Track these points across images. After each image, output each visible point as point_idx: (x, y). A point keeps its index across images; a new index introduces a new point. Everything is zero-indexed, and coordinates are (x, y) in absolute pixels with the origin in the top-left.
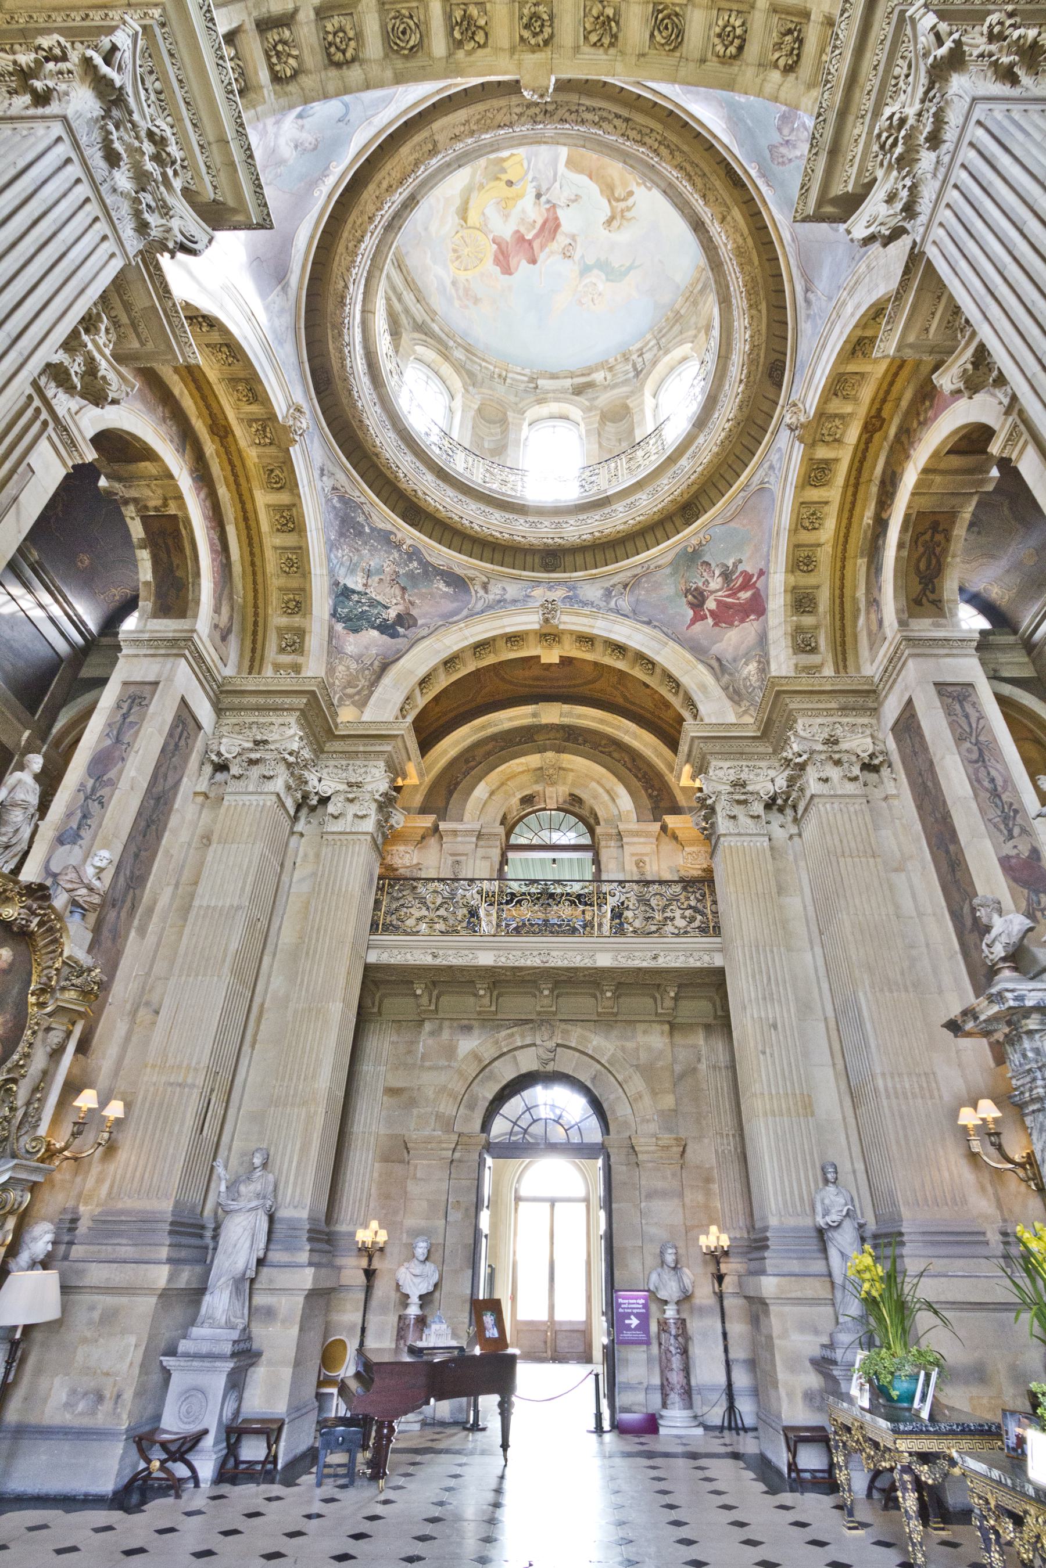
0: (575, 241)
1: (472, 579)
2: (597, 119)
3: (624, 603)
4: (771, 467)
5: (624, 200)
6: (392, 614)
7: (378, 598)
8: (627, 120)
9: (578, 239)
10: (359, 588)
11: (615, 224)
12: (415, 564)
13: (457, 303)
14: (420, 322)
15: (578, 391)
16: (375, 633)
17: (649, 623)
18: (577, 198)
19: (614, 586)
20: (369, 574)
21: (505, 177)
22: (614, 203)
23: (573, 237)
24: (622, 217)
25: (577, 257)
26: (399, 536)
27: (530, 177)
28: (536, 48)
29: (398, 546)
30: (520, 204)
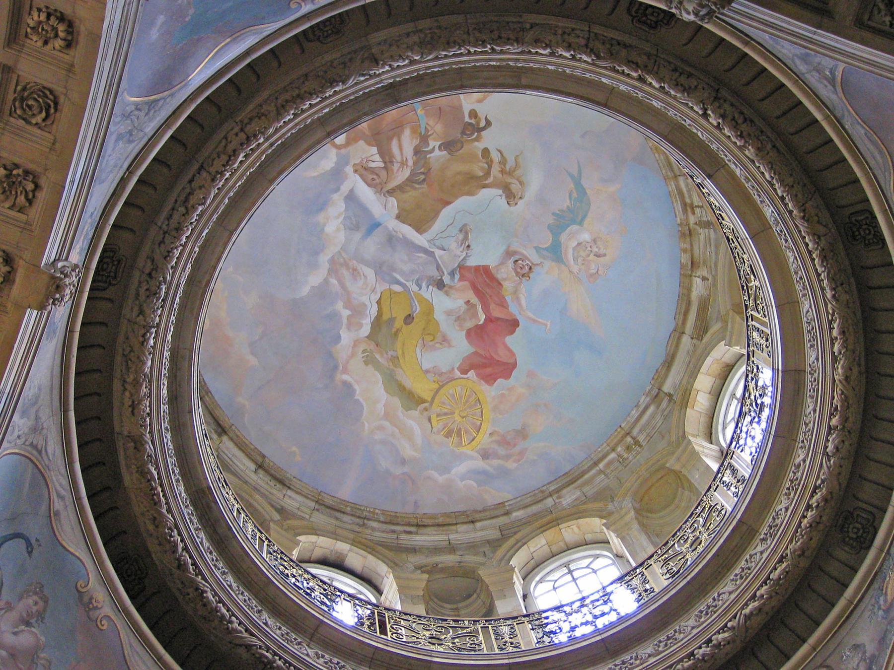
0: (515, 253)
2: (182, 210)
4: (805, 59)
5: (490, 164)
8: (202, 167)
9: (515, 247)
11: (515, 187)
13: (511, 465)
14: (496, 534)
15: (702, 329)
18: (464, 230)
21: (399, 323)
22: (490, 180)
23: (509, 254)
24: (510, 173)
25: (534, 257)
27: (415, 288)
30: (439, 315)
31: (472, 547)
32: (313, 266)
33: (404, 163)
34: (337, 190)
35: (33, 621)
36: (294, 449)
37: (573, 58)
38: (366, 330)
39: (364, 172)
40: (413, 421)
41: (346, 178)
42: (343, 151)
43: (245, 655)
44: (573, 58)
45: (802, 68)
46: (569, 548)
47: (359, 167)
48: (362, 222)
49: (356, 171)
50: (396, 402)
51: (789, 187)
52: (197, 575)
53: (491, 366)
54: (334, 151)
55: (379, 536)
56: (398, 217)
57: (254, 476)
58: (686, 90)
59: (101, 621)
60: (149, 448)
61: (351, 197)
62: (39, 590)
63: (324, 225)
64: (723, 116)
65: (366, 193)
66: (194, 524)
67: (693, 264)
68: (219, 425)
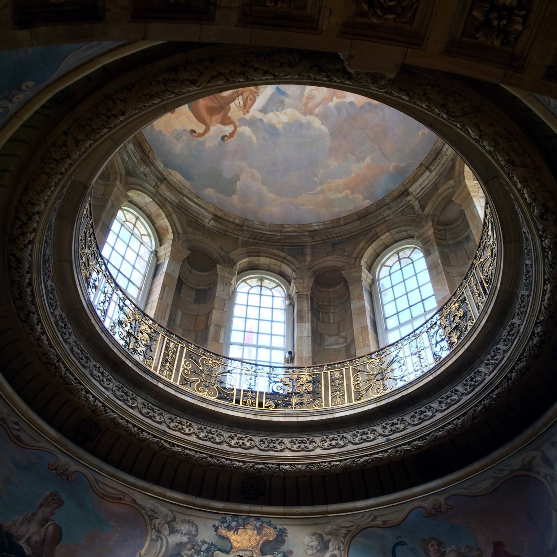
32: (309, 125)
34: (261, 120)
35: (443, 550)
36: (420, 133)
39: (247, 106)
41: (253, 116)
42: (237, 124)
47: (245, 111)
49: (248, 112)
52: (426, 439)
54: (239, 129)
57: (434, 173)
59: (448, 506)
61: (264, 110)
63: (283, 123)
68: (403, 193)
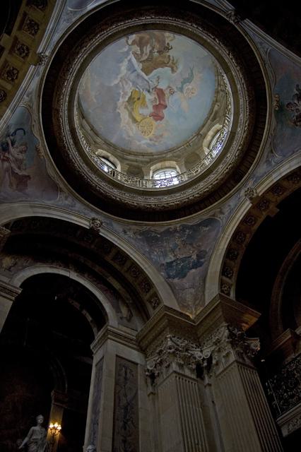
1: (214, 215)
3: (278, 157)
4: (261, 44)
5: (170, 59)
6: (194, 257)
7: (184, 256)
9: (171, 85)
10: (173, 259)
12: (188, 231)
13: (156, 144)
14: (149, 160)
15: (214, 119)
16: (194, 270)
17: (294, 152)
18: (158, 77)
19: (267, 157)
20: (173, 251)
21: (136, 100)
23: (169, 87)
25: (175, 90)
26: (172, 227)
28: (27, 55)
29: (175, 231)
30: (147, 100)
31: (142, 162)
33: (146, 54)
34: (126, 58)
37: (197, 28)
38: (127, 99)
40: (134, 127)
43: (77, 173)
44: (197, 28)
45: (259, 46)
46: (166, 168)
48: (131, 69)
50: (131, 120)
51: (246, 81)
53: (157, 116)
54: (127, 47)
55: (119, 154)
56: (142, 70)
58: (226, 45)
60: (61, 114)
61: (130, 61)
62: (26, 144)
64: (234, 56)
65: (134, 60)
66: (69, 137)
67: (217, 101)
